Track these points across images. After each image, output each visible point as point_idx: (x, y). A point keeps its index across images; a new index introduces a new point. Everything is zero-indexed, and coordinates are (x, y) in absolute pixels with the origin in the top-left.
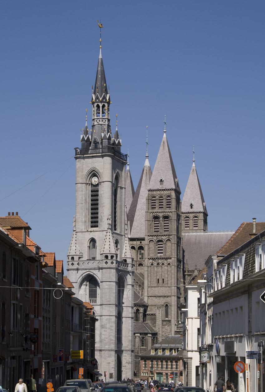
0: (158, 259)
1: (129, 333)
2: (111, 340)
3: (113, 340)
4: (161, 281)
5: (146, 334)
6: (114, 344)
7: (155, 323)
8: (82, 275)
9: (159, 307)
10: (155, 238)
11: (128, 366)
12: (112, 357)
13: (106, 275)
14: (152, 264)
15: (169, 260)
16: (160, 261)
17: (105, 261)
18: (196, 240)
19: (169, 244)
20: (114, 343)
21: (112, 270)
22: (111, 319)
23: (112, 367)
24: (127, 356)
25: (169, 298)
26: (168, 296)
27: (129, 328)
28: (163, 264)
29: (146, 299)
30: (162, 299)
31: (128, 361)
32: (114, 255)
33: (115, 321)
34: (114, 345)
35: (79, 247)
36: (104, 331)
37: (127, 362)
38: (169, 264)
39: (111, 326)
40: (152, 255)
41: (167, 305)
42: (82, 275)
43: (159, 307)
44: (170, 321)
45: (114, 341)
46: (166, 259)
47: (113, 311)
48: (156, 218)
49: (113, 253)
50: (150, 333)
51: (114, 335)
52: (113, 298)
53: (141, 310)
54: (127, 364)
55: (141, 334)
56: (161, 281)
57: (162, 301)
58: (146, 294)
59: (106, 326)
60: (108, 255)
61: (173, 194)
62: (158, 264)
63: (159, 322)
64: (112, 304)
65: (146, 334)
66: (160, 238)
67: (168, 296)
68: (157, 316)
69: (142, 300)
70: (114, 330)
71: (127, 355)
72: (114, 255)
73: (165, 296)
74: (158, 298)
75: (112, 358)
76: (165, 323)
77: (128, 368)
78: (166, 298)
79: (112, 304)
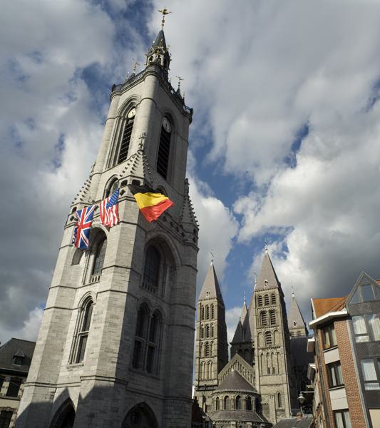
0: (267, 348)
1: (180, 359)
2: (108, 350)
3: (112, 351)
4: (271, 370)
5: (259, 423)
6: (113, 362)
7: (268, 413)
9: (271, 396)
10: (263, 330)
12: (103, 399)
14: (262, 354)
15: (278, 350)
16: (269, 351)
19: (276, 334)
20: (116, 360)
22: (116, 300)
24: (173, 412)
25: (281, 387)
26: (280, 385)
27: (181, 348)
28: (272, 353)
29: (258, 388)
30: (273, 387)
32: (140, 180)
33: (124, 305)
34: (115, 365)
36: (95, 328)
38: (278, 353)
39: (112, 317)
40: (261, 346)
41: (279, 394)
43: (271, 396)
44: (283, 411)
45: (117, 355)
46: (275, 348)
47: (123, 282)
48: (263, 313)
50: (263, 423)
51: (119, 338)
53: (253, 399)
55: (253, 423)
56: (271, 370)
57: (274, 390)
58: (257, 383)
60: (128, 179)
61: (277, 291)
62: (268, 353)
63: (272, 412)
64: (121, 267)
65: (259, 423)
66: (268, 330)
67: (280, 385)
68: (270, 406)
69: (254, 389)
70: (121, 327)
71: (172, 408)
72: (140, 180)
73: (277, 385)
74: (270, 387)
76: (278, 413)
78: (277, 387)
79: (121, 267)
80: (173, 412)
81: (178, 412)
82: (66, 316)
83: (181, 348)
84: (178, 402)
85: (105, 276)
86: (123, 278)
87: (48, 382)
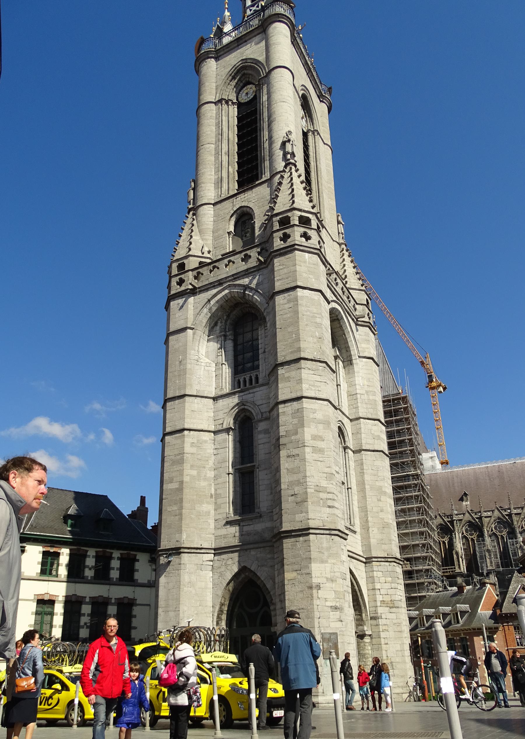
1: (379, 500)
8: (209, 301)
11: (390, 616)
12: (326, 562)
13: (285, 271)
17: (280, 234)
18: (431, 480)
21: (307, 254)
23: (329, 604)
24: (382, 580)
27: (378, 484)
31: (387, 599)
35: (203, 240)
36: (288, 456)
37: (383, 602)
42: (209, 301)
47: (319, 384)
49: (306, 209)
52: (315, 340)
54: (388, 608)
59: (293, 438)
64: (312, 360)
71: (380, 574)
75: (328, 566)
77: (388, 622)
79: (312, 360)
80: (382, 580)
81: (390, 579)
82: (206, 442)
83: (378, 484)
84: (387, 564)
85: (287, 375)
86: (318, 378)
87: (199, 546)
